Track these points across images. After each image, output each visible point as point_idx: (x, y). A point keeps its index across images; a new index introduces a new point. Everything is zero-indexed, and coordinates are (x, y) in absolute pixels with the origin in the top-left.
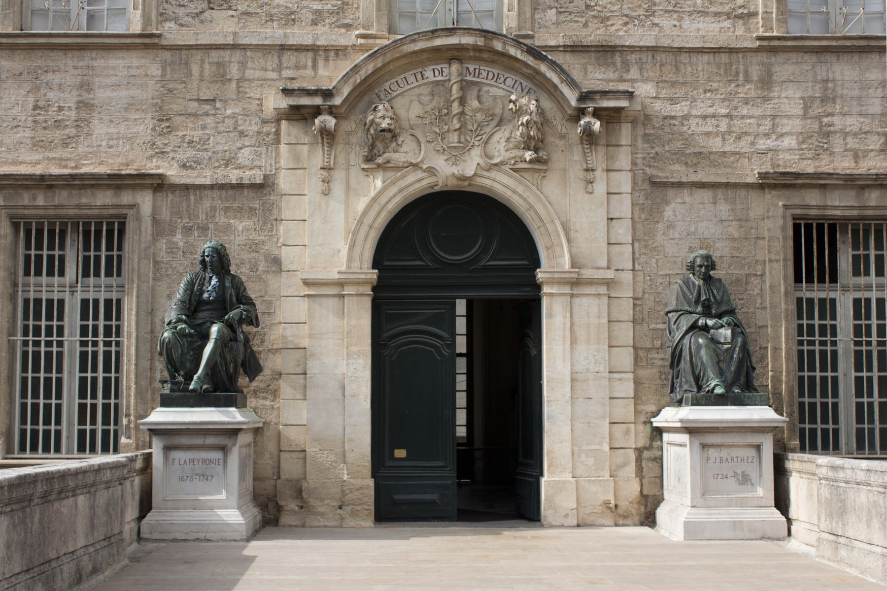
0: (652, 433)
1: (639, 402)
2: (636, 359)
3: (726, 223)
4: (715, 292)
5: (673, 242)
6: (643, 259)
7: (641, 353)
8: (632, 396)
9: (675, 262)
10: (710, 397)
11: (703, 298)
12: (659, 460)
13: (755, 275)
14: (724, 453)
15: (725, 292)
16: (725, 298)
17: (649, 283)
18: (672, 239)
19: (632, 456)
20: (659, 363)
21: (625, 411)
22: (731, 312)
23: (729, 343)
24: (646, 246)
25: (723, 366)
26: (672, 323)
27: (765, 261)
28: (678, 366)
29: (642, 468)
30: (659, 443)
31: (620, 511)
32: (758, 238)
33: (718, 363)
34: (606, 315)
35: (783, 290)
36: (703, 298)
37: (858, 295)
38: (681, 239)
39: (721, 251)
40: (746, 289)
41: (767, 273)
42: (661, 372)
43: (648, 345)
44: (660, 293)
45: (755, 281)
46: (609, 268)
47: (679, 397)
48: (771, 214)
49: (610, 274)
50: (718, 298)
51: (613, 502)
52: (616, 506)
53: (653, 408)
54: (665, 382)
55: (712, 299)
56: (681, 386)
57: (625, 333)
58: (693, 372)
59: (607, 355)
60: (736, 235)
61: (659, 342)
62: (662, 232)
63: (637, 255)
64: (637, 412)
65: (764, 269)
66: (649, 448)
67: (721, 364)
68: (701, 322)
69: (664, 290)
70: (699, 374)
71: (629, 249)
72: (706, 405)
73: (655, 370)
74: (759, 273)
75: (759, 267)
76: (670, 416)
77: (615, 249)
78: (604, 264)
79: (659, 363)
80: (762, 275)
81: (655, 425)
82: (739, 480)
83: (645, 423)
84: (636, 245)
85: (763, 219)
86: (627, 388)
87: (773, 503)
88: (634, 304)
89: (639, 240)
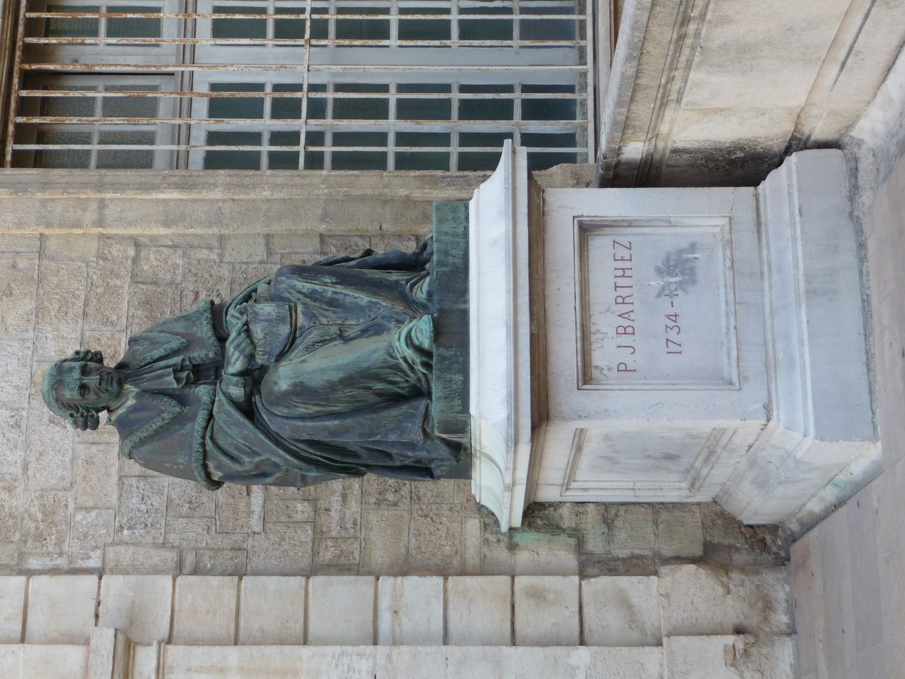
0: (537, 529)
1: (456, 562)
2: (341, 567)
4: (156, 354)
5: (32, 466)
6: (72, 546)
7: (327, 555)
8: (439, 580)
9: (89, 462)
10: (443, 358)
11: (170, 381)
12: (609, 513)
13: (135, 260)
14: (604, 323)
15: (163, 327)
16: (179, 327)
17: (139, 531)
18: (25, 468)
19: (600, 584)
20: (354, 506)
21: (479, 602)
22: (217, 313)
23: (292, 310)
24: (40, 537)
25: (355, 325)
26: (236, 467)
27: (102, 236)
28: (355, 455)
29: (633, 557)
30: (565, 511)
31: (753, 621)
32: (41, 252)
33: (346, 340)
34: (216, 650)
35: (175, 195)
36: (170, 381)
37: (205, 27)
38: (28, 445)
39: (63, 342)
40: (170, 284)
41: (132, 231)
42: (378, 503)
43: (306, 535)
44: (169, 500)
46: (87, 642)
47: (444, 452)
49: (104, 639)
50: (175, 344)
51: (730, 639)
52: (739, 631)
53: (473, 525)
54: (405, 491)
55: (177, 360)
56: (412, 446)
57: (270, 597)
58: (372, 408)
59: (328, 649)
60: (29, 305)
61: (299, 506)
63: (62, 562)
64: (483, 570)
65: (121, 239)
66: (578, 536)
67: (351, 333)
68: (237, 392)
69: (160, 492)
70: (379, 394)
71: (37, 582)
72: (465, 370)
73: (373, 518)
74: (131, 252)
76: (496, 482)
77: (36, 623)
78: (74, 655)
79: (354, 506)
80: (137, 245)
81: (517, 521)
82: (681, 284)
83: (512, 547)
84: (34, 563)
86: (420, 594)
87: (746, 192)
88: (195, 572)
89: (22, 556)
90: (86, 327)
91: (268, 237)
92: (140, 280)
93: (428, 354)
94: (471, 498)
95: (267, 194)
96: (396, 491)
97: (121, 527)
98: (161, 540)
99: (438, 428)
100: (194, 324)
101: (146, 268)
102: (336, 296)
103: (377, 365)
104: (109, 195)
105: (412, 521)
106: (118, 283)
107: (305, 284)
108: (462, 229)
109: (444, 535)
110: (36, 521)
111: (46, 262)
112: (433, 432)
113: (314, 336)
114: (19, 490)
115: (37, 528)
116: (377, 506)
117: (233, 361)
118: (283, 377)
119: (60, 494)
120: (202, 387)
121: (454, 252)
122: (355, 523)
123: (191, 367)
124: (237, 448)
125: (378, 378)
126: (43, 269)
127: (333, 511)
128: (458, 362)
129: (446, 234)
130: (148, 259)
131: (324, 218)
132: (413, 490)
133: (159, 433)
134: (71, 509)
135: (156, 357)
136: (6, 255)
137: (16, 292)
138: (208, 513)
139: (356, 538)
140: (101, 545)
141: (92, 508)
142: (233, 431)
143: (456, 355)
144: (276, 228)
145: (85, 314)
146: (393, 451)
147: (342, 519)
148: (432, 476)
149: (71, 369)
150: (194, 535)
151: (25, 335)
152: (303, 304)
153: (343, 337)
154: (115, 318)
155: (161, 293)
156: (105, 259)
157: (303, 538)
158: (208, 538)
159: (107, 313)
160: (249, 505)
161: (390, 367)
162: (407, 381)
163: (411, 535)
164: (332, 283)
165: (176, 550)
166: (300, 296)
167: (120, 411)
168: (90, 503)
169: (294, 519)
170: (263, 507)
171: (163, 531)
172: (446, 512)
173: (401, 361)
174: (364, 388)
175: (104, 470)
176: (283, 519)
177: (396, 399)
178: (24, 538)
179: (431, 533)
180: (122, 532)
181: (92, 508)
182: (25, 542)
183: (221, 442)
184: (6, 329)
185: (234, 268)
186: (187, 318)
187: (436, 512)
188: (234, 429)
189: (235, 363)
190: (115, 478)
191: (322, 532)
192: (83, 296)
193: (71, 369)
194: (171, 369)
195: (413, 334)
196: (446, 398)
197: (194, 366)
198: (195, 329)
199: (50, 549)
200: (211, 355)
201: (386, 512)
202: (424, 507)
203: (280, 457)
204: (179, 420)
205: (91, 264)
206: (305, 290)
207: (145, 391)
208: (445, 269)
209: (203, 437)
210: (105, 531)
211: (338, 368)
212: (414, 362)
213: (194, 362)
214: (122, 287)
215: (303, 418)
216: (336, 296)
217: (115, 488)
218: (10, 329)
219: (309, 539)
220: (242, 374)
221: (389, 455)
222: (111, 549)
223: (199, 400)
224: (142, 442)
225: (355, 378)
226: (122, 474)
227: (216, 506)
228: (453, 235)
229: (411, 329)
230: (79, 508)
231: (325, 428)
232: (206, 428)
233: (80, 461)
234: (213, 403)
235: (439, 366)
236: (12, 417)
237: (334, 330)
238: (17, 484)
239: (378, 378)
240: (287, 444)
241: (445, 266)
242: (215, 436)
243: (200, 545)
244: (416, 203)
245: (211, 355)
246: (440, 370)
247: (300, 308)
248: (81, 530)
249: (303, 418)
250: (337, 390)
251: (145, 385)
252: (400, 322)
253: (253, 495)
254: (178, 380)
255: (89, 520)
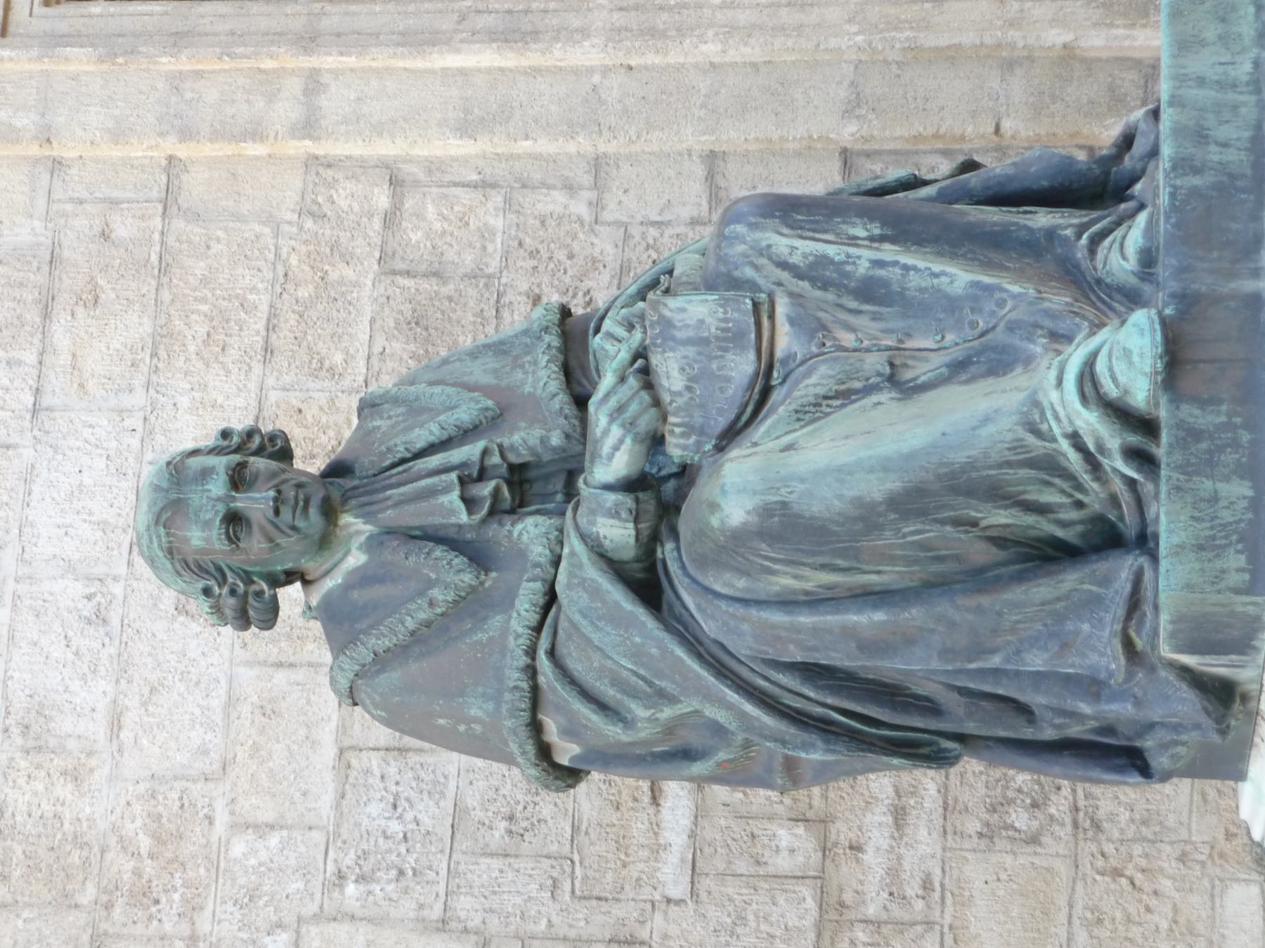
3: (58, 388)
4: (421, 436)
5: (129, 719)
9: (268, 710)
10: (1191, 434)
11: (450, 508)
13: (391, 220)
15: (440, 373)
16: (480, 372)
17: (385, 887)
18: (116, 725)
20: (925, 838)
23: (762, 312)
24: (144, 897)
25: (930, 348)
26: (614, 732)
27: (312, 162)
28: (931, 707)
32: (168, 202)
36: (450, 508)
38: (123, 671)
40: (471, 276)
41: (385, 148)
44: (459, 811)
45: (427, 223)
47: (1187, 703)
48: (25, 121)
50: (465, 414)
54: (1059, 806)
55: (469, 452)
56: (1093, 686)
58: (979, 579)
60: (138, 326)
61: (785, 836)
62: (64, 790)
67: (921, 371)
68: (618, 533)
69: (436, 790)
70: (999, 542)
73: (974, 872)
74: (382, 199)
75: (345, 195)
80: (395, 182)
85: (57, 164)
90: (270, 381)
91: (712, 159)
92: (400, 266)
93: (1148, 427)
94: (1236, 830)
95: (711, 49)
96: (1035, 805)
97: (341, 876)
98: (436, 912)
99: (1173, 635)
100: (517, 365)
101: (415, 237)
102: (882, 273)
103: (995, 457)
104: (329, 61)
105: (1079, 886)
106: (349, 273)
107: (798, 243)
108: (1248, 67)
109: (1164, 925)
110: (136, 855)
111: (178, 224)
112: (1154, 647)
113: (818, 380)
114: (100, 777)
115: (137, 873)
116: (983, 843)
117: (606, 449)
118: (733, 493)
119: (197, 789)
120: (530, 521)
121: (1223, 133)
122: (927, 885)
123: (504, 470)
124: (616, 682)
125: (996, 494)
126: (171, 241)
127: (870, 850)
128: (1235, 444)
129: (1201, 81)
130: (419, 216)
131: (854, 106)
132: (1081, 803)
133: (421, 640)
134: (220, 827)
135: (420, 444)
136: (87, 207)
137: (107, 296)
138: (554, 848)
139: (929, 924)
140: (290, 919)
141: (272, 827)
142: (606, 637)
143: (1229, 426)
144: (731, 136)
145: (268, 350)
146: (1036, 699)
147: (894, 872)
148: (1145, 770)
149: (206, 473)
150: (518, 900)
151: (127, 401)
152: (791, 295)
153: (896, 381)
154: (338, 358)
155: (450, 299)
156: (320, 217)
157: (793, 921)
158: (551, 909)
159: (321, 347)
160: (655, 828)
161: (1031, 464)
162: (1079, 505)
163: (1076, 922)
164: (872, 239)
165: (473, 938)
166: (785, 276)
167: (329, 583)
168: (268, 816)
169: (771, 870)
170: (692, 835)
171: (441, 888)
172: (1171, 866)
173: (1065, 445)
174: (958, 522)
175: (302, 732)
176: (742, 866)
177: (1051, 554)
178: (105, 898)
179: (1129, 920)
180: (341, 887)
181: (272, 827)
182: (109, 906)
183: (576, 666)
184: (81, 386)
185: (627, 236)
186: (499, 348)
187: (1143, 863)
188: (607, 627)
189: (611, 457)
190: (329, 752)
191: (842, 904)
192: (264, 308)
193: (206, 473)
194: (453, 476)
195: (1101, 367)
196: (1201, 548)
197: (512, 468)
198: (519, 375)
199: (168, 927)
200: (556, 440)
201: (1008, 860)
202: (1109, 848)
203: (727, 707)
204: (471, 606)
205: (285, 228)
206: (796, 259)
207: (390, 532)
208: (1197, 181)
209: (532, 652)
210: (300, 885)
211: (885, 466)
212: (1101, 448)
213: (513, 458)
214: (356, 284)
215: (787, 602)
216: (882, 273)
217: (329, 776)
218: (91, 385)
219: (809, 921)
220: (634, 485)
221: (1024, 711)
222: (314, 930)
223: (521, 554)
224: (381, 661)
225: (930, 494)
226: (347, 743)
227: (575, 829)
228: (1221, 85)
229: (1094, 355)
230: (240, 826)
231: (848, 633)
232: (538, 629)
233: (245, 709)
234: (556, 562)
235: (1178, 457)
236: (89, 597)
237: (875, 363)
238: (93, 762)
239: (996, 494)
240: (745, 673)
241: (1197, 171)
242: (562, 650)
243: (531, 927)
244: (1090, 64)
245: (556, 440)
246: (1182, 468)
247: (782, 308)
248: (242, 881)
249: (787, 602)
250: (880, 528)
251: (389, 516)
252: (1060, 338)
253: (666, 804)
254: (470, 503)
255: (264, 855)
